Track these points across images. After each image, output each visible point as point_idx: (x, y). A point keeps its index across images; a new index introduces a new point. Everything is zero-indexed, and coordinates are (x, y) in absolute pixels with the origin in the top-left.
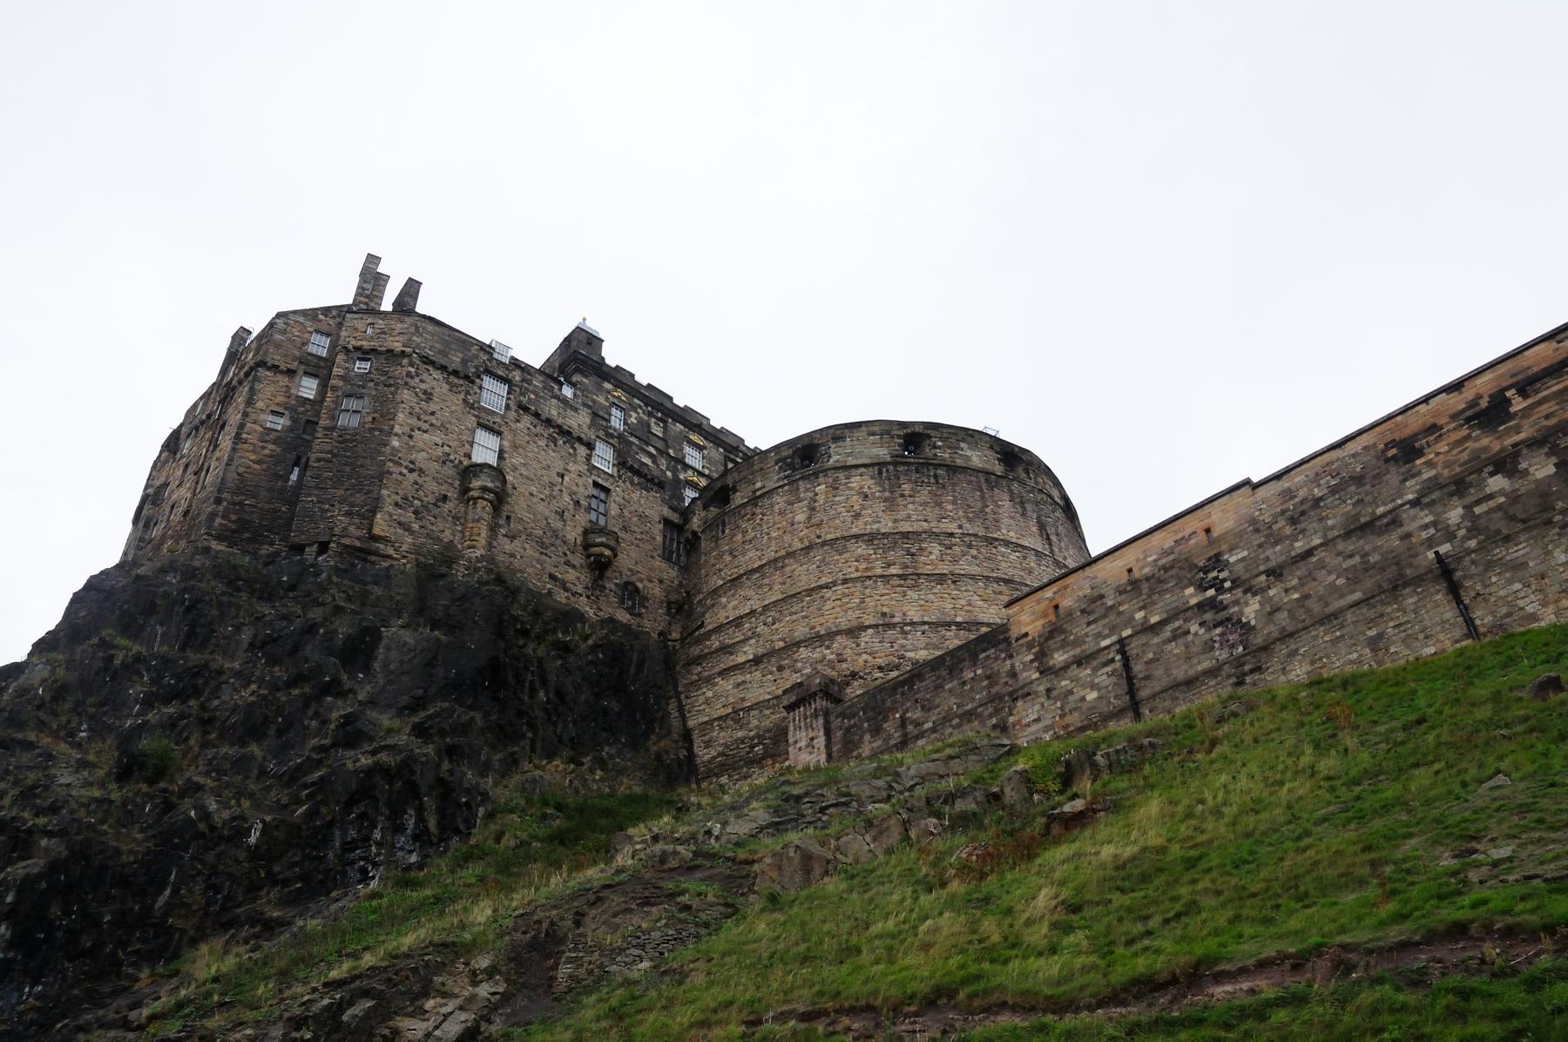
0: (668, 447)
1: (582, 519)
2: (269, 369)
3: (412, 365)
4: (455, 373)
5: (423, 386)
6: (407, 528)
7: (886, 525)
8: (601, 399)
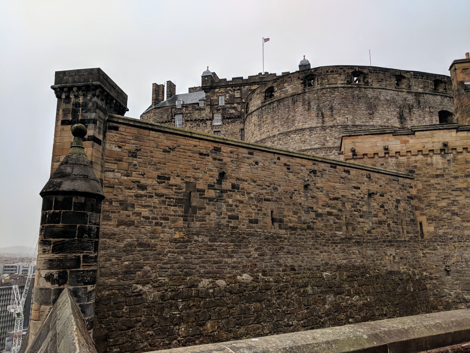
4: (166, 122)
8: (215, 98)
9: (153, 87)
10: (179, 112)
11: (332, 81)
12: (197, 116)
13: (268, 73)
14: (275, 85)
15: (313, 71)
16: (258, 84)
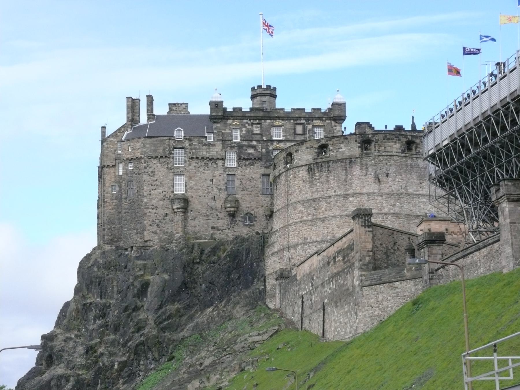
0: (262, 136)
1: (224, 195)
2: (107, 167)
3: (145, 163)
4: (162, 157)
5: (151, 170)
6: (155, 233)
7: (309, 196)
8: (228, 131)
9: (127, 102)
10: (179, 146)
11: (388, 149)
12: (205, 153)
13: (270, 86)
14: (330, 143)
15: (370, 136)
16: (283, 120)
